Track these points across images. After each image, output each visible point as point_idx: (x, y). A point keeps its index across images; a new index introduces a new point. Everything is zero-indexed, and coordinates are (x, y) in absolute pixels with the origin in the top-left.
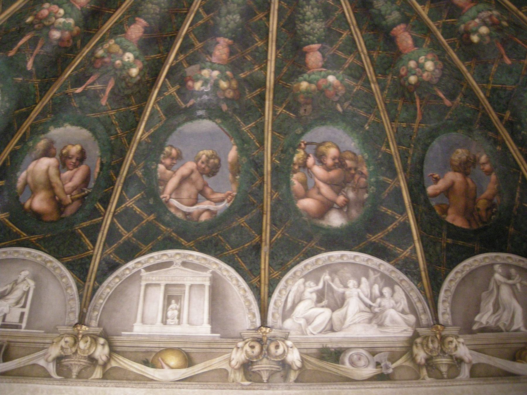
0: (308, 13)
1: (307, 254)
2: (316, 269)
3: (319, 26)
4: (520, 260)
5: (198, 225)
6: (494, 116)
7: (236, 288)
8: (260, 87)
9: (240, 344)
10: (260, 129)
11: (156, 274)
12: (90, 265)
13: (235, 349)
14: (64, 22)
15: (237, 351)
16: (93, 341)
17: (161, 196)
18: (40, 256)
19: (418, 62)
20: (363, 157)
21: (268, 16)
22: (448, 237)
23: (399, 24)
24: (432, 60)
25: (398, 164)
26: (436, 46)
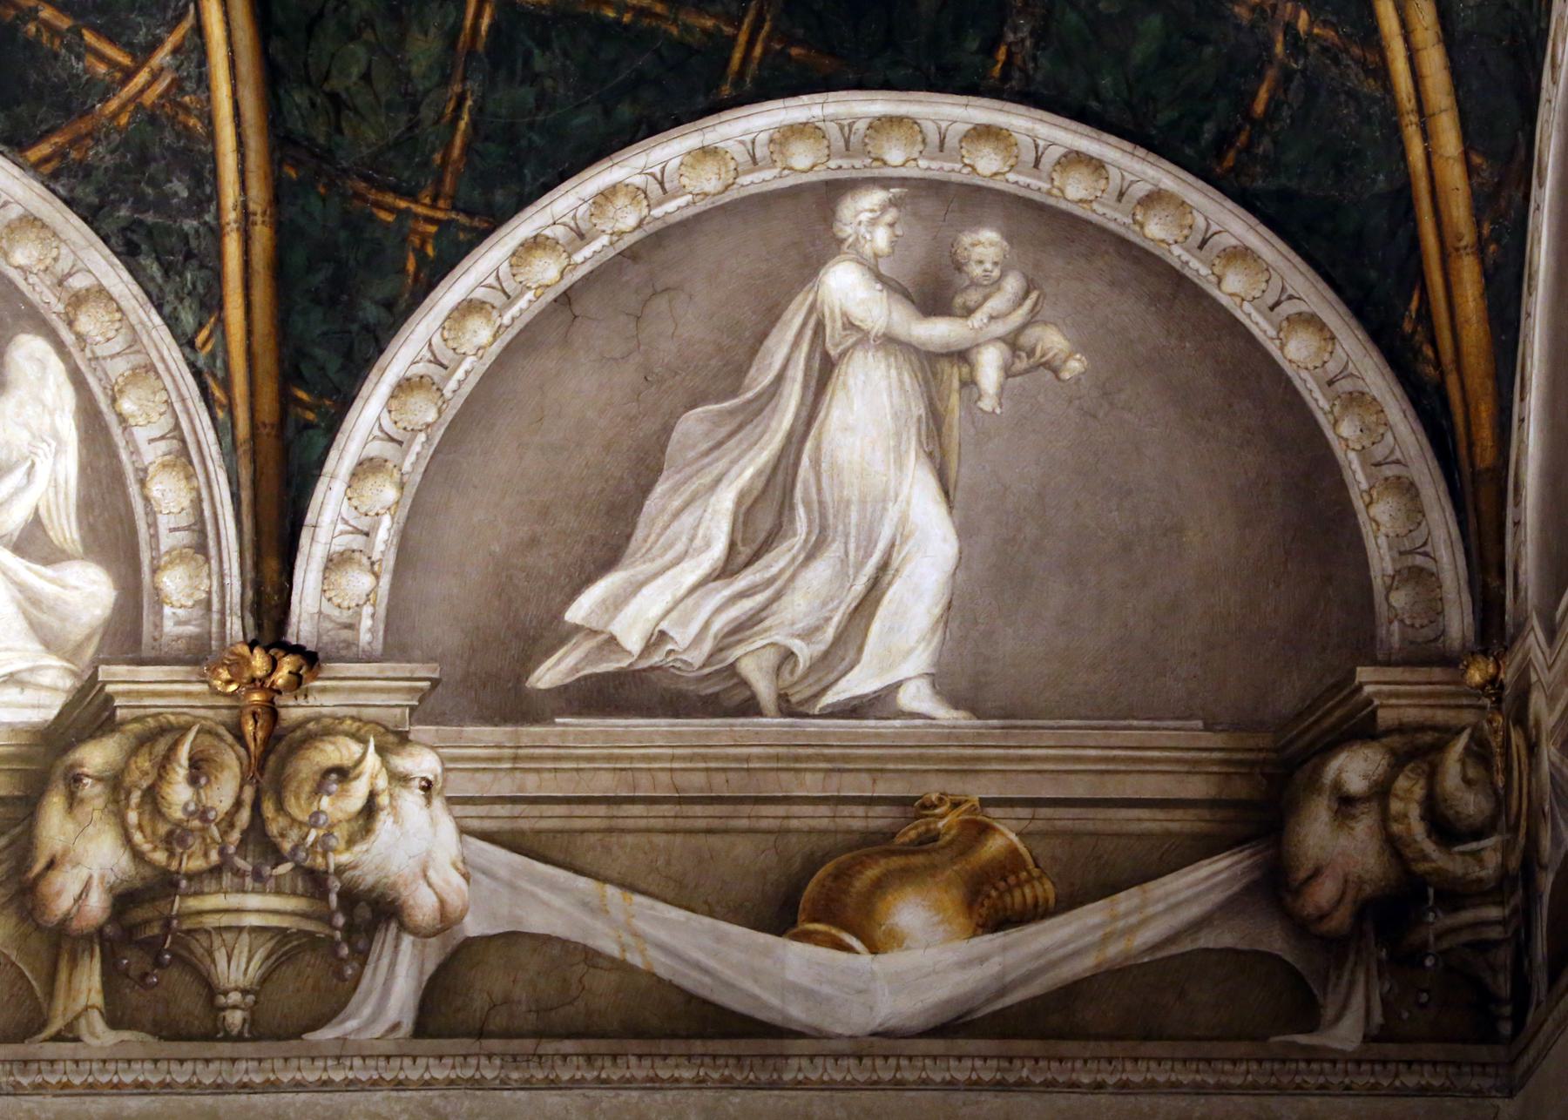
4: (1075, 159)
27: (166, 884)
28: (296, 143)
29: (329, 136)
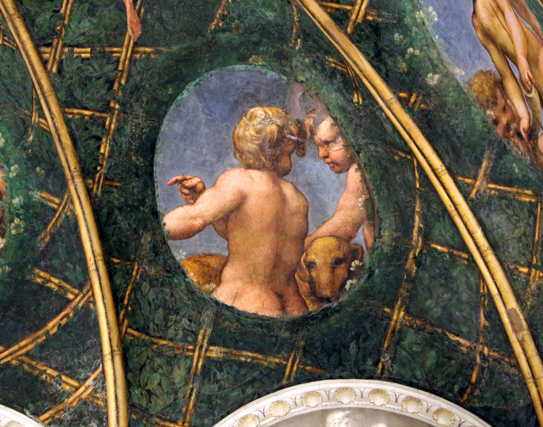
4: (410, 399)
22: (212, 343)
28: (135, 407)
29: (147, 404)
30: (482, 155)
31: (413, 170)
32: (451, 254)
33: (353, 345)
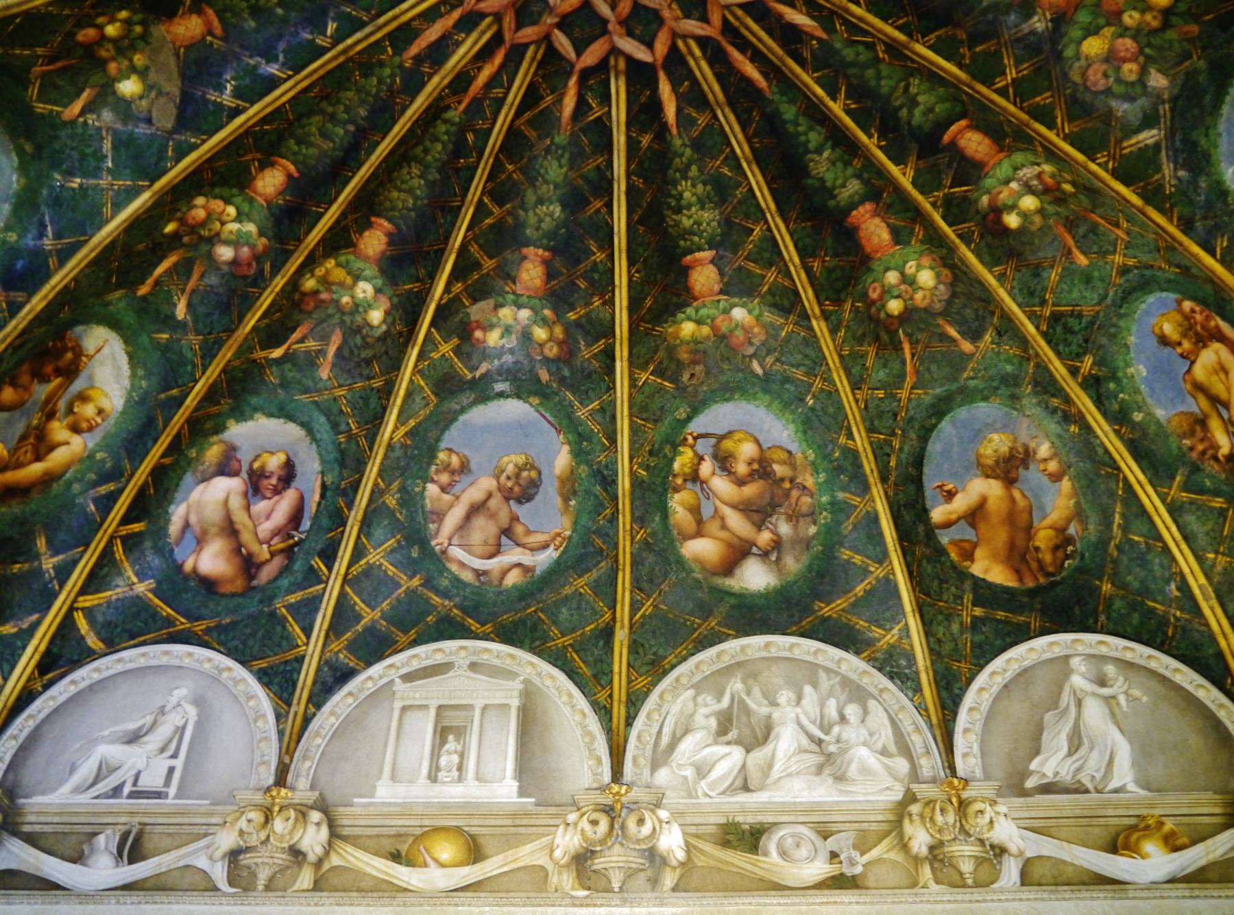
0: (687, 195)
1: (700, 642)
2: (718, 671)
3: (708, 218)
4: (1126, 648)
5: (500, 593)
6: (1058, 368)
7: (567, 711)
8: (604, 336)
9: (572, 817)
10: (608, 413)
11: (422, 686)
12: (299, 673)
13: (562, 827)
14: (239, 231)
15: (566, 830)
16: (300, 817)
17: (433, 543)
18: (210, 660)
19: (903, 274)
20: (806, 458)
21: (609, 205)
22: (974, 605)
23: (862, 202)
24: (932, 268)
25: (869, 466)
26: (935, 241)
27: (941, 844)
30: (1177, 471)
31: (1118, 482)
32: (1147, 543)
33: (1077, 610)
